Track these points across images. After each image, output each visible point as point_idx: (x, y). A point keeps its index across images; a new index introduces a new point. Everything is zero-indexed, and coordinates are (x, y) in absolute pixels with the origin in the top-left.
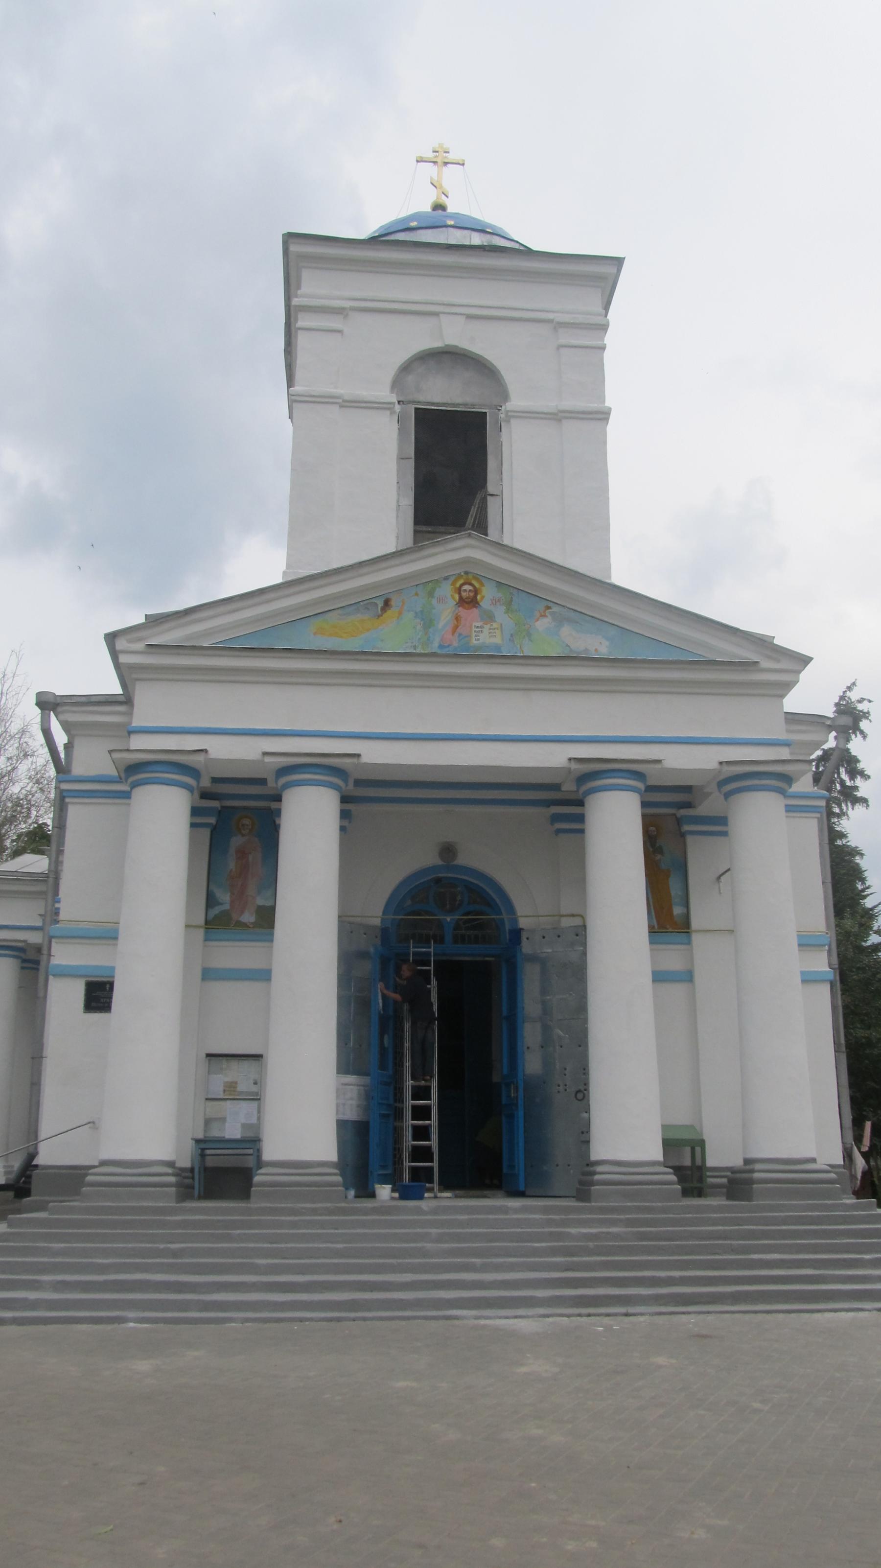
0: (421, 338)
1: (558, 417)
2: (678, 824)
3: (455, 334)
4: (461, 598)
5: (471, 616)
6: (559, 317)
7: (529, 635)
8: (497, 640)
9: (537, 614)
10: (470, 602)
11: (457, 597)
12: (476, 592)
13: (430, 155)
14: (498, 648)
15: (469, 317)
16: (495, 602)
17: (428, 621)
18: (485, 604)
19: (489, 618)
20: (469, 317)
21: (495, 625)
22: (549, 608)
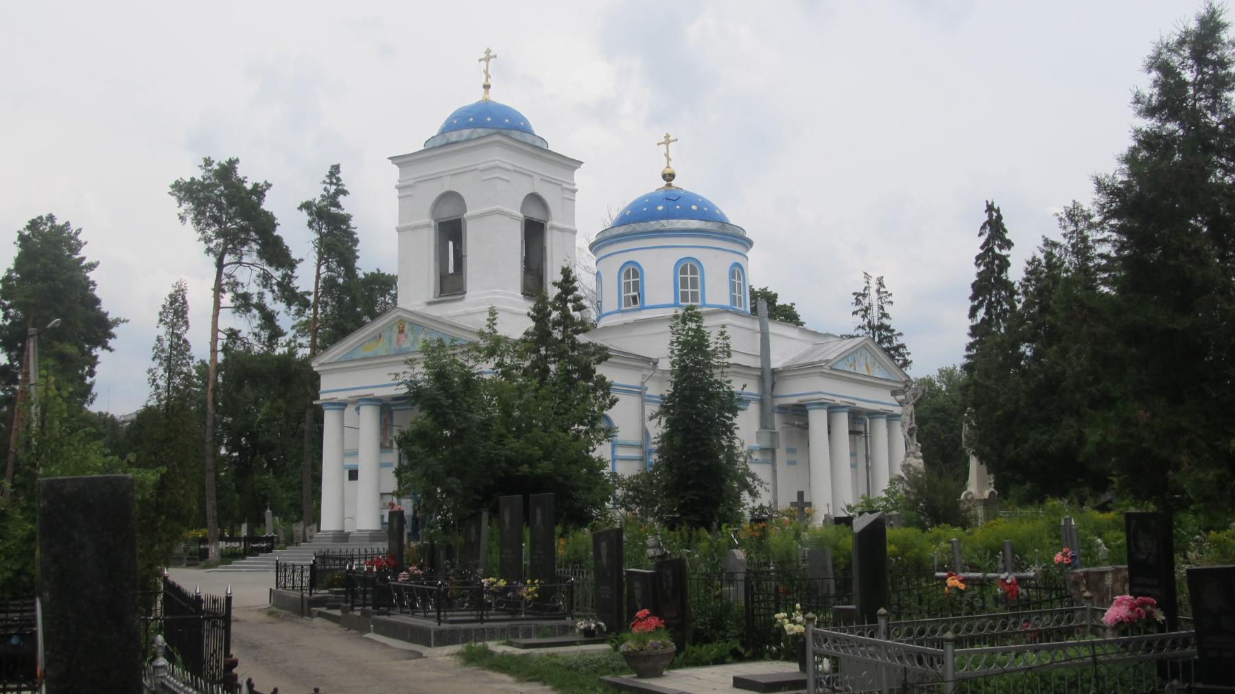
0: (437, 190)
10: (401, 331)
13: (484, 56)
17: (391, 342)
19: (407, 337)
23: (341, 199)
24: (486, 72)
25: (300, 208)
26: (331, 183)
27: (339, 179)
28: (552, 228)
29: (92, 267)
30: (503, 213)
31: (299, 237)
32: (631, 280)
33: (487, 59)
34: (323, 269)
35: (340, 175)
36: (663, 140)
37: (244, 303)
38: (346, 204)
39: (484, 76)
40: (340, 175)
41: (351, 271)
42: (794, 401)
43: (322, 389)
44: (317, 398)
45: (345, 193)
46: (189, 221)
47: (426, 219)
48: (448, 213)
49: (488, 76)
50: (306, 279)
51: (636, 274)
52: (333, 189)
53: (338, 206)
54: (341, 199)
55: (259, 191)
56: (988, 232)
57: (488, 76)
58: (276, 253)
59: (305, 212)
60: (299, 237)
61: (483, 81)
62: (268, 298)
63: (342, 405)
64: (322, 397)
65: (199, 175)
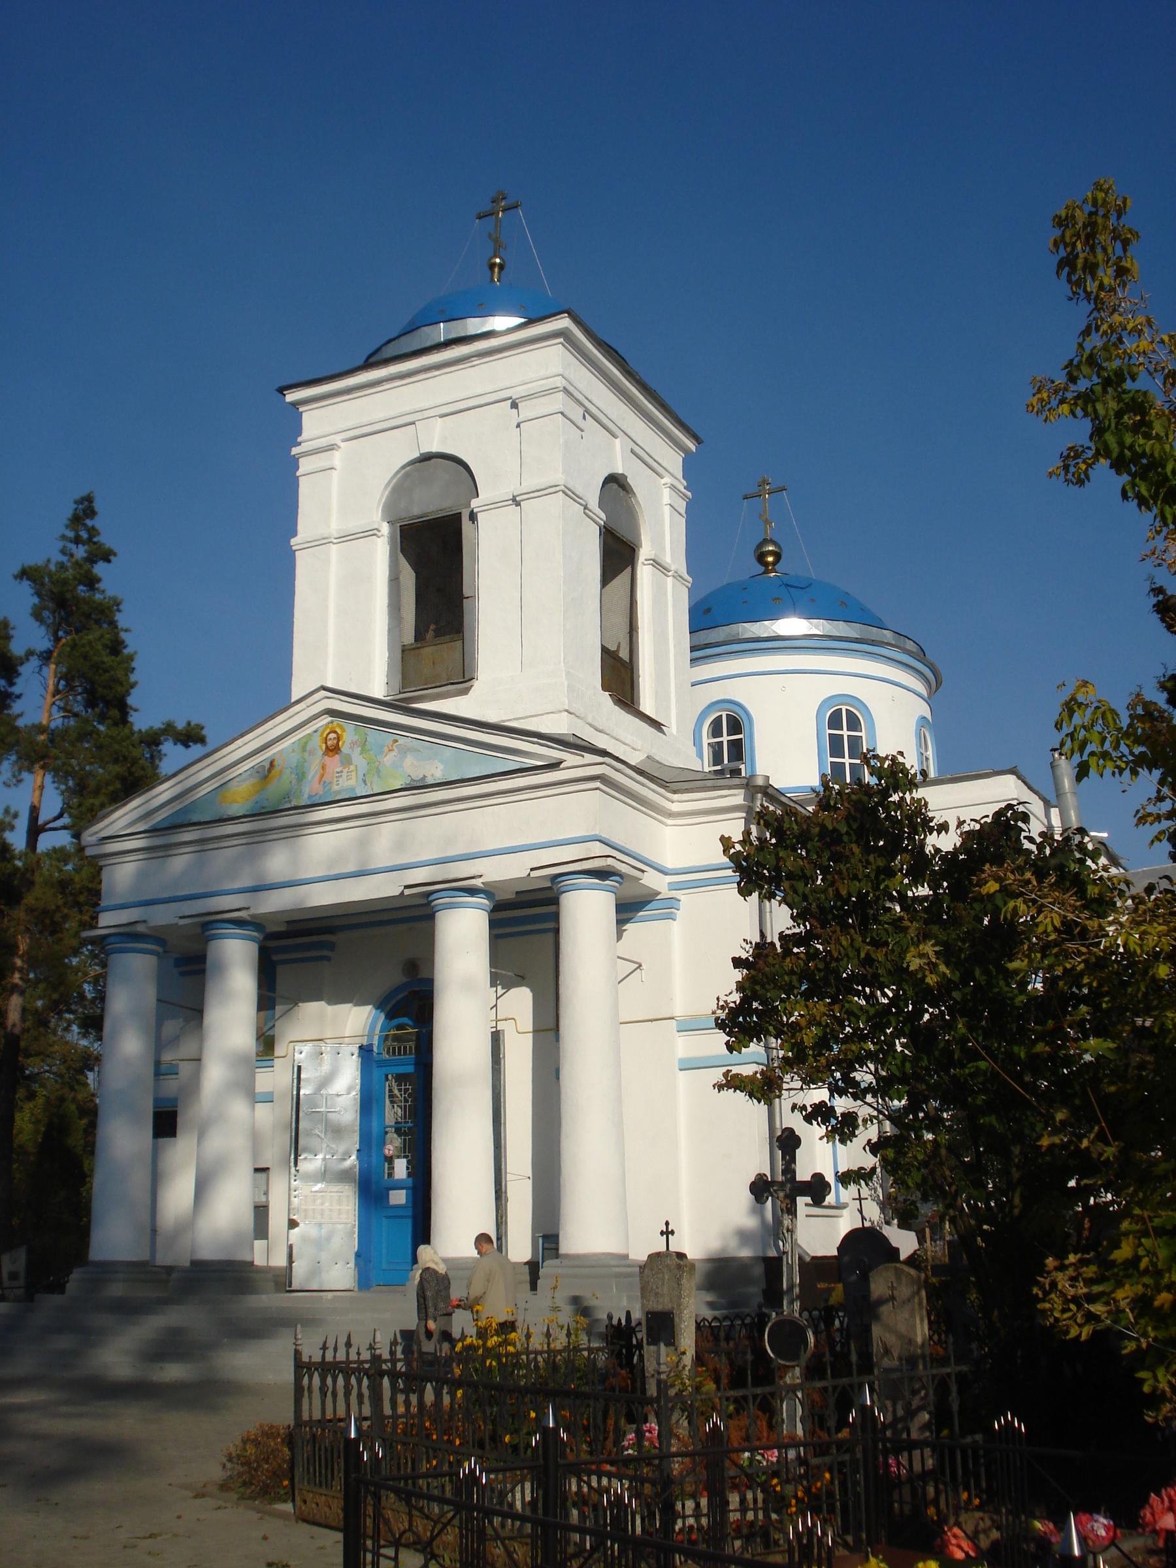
0: (399, 451)
2: (526, 924)
4: (327, 747)
5: (334, 762)
6: (515, 393)
7: (378, 771)
8: (352, 782)
9: (386, 749)
10: (333, 750)
11: (324, 746)
12: (338, 739)
14: (353, 789)
16: (353, 744)
18: (345, 749)
19: (347, 761)
21: (352, 768)
22: (396, 741)
23: (100, 569)
26: (77, 541)
27: (93, 532)
32: (725, 738)
35: (96, 522)
36: (755, 489)
38: (112, 579)
40: (96, 522)
48: (429, 503)
51: (735, 726)
52: (80, 552)
53: (92, 582)
54: (100, 569)
59: (26, 587)
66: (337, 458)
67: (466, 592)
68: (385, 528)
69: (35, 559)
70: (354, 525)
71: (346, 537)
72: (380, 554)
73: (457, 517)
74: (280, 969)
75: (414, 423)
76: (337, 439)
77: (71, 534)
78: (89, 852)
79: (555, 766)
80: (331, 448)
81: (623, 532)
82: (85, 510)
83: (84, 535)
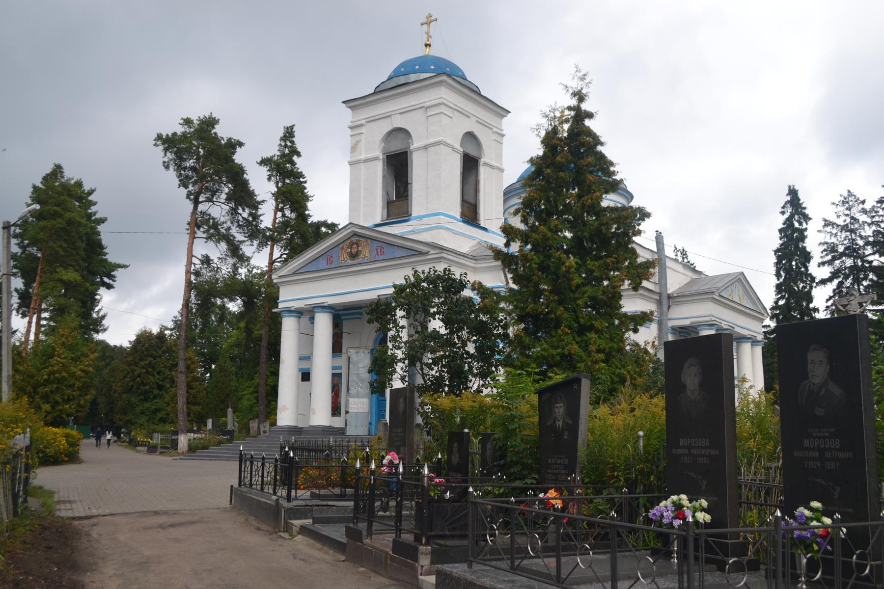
1: (426, 147)
3: (398, 122)
6: (425, 105)
13: (425, 20)
15: (401, 113)
20: (401, 113)
23: (295, 158)
24: (427, 33)
25: (264, 162)
27: (293, 142)
28: (485, 164)
29: (91, 192)
30: (447, 145)
31: (262, 185)
33: (428, 23)
34: (279, 214)
35: (294, 139)
37: (215, 233)
39: (425, 36)
40: (294, 139)
41: (302, 216)
42: (687, 322)
43: (281, 299)
44: (276, 305)
45: (299, 154)
46: (172, 168)
47: (378, 153)
48: (396, 146)
49: (429, 37)
50: (267, 217)
53: (293, 163)
54: (295, 158)
55: (233, 145)
56: (789, 210)
57: (429, 37)
58: (242, 196)
60: (262, 185)
61: (425, 41)
62: (234, 231)
63: (299, 313)
64: (281, 306)
65: (180, 130)
66: (363, 130)
67: (409, 181)
68: (381, 157)
69: (267, 154)
70: (369, 156)
71: (367, 161)
72: (379, 168)
73: (406, 152)
74: (344, 322)
75: (390, 116)
76: (363, 122)
77: (283, 144)
78: (275, 281)
79: (427, 253)
80: (361, 125)
81: (472, 152)
82: (289, 134)
83: (289, 144)
